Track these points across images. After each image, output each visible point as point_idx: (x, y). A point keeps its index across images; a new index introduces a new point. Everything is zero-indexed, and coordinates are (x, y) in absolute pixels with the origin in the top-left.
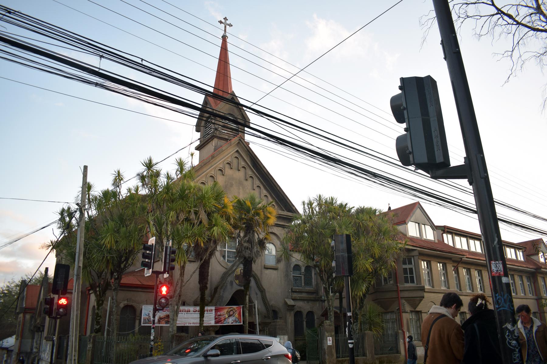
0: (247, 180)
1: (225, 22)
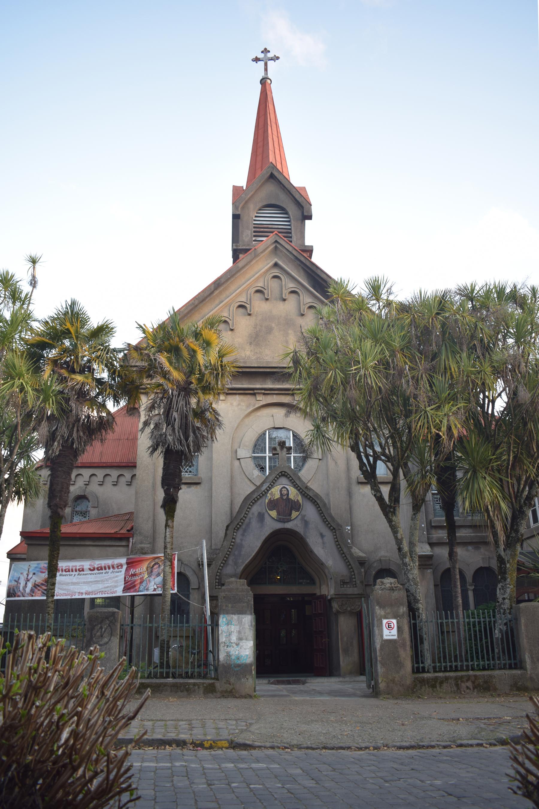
0: (303, 315)
1: (265, 58)
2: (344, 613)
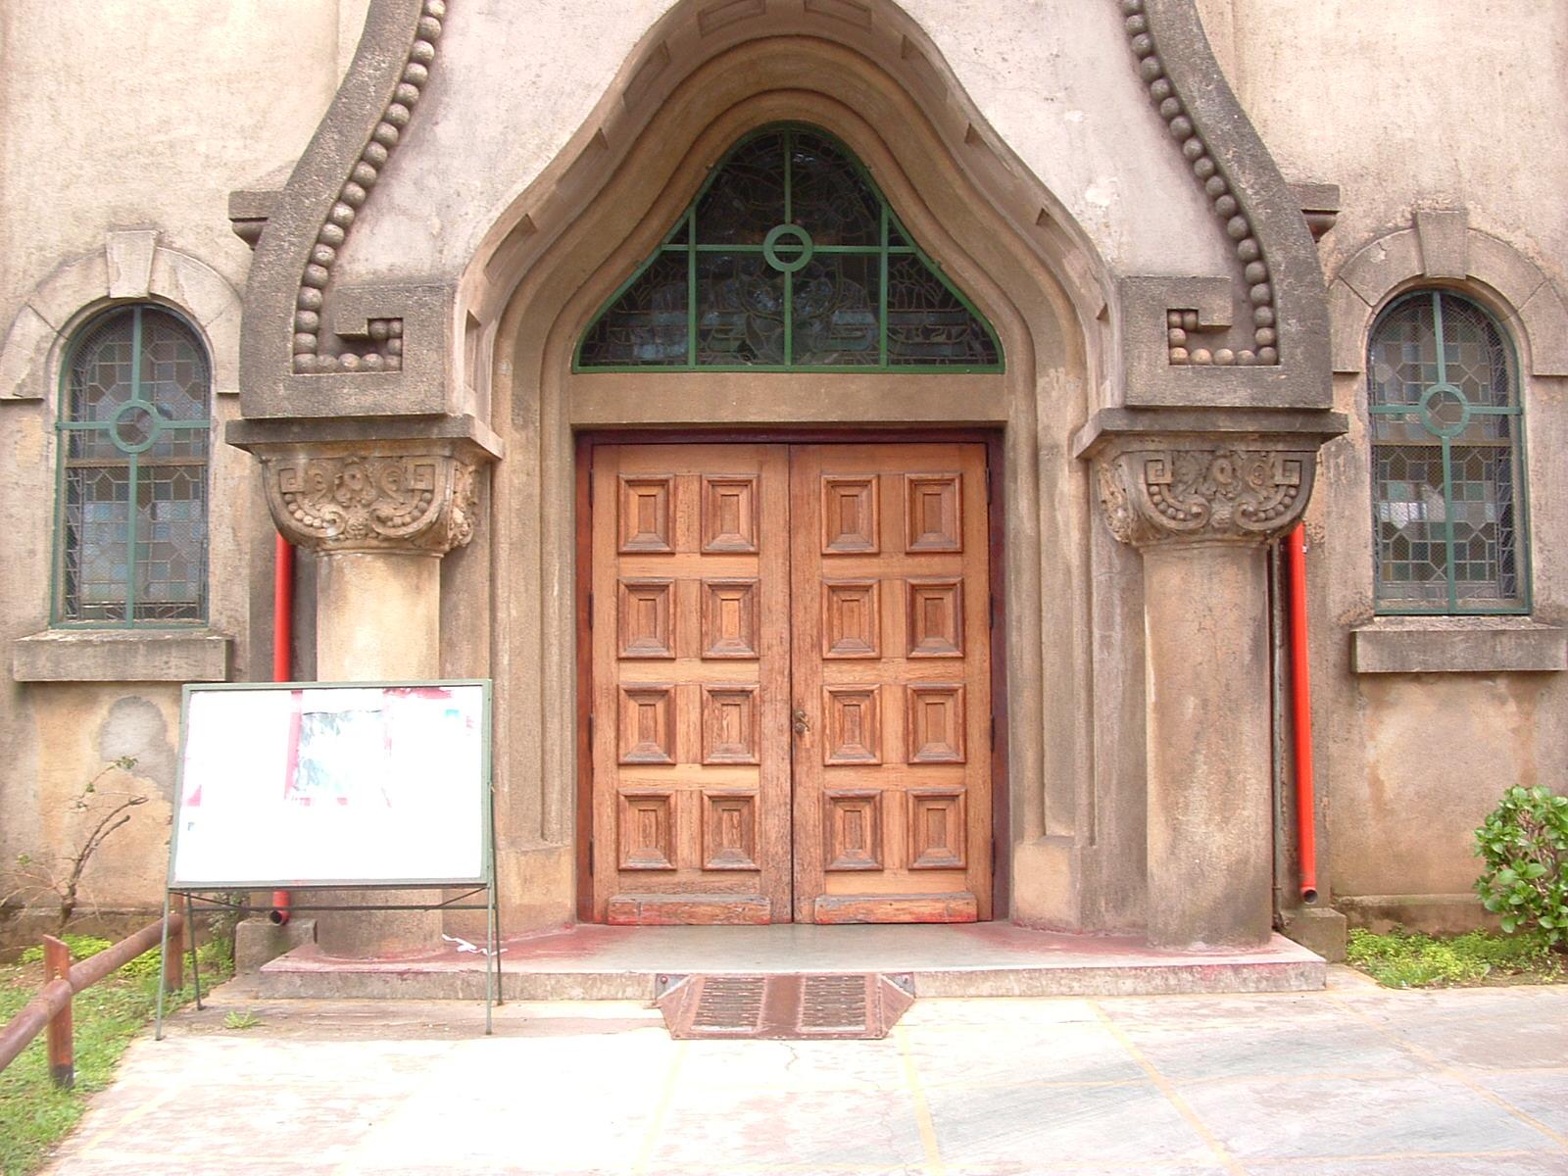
2: (1182, 538)
